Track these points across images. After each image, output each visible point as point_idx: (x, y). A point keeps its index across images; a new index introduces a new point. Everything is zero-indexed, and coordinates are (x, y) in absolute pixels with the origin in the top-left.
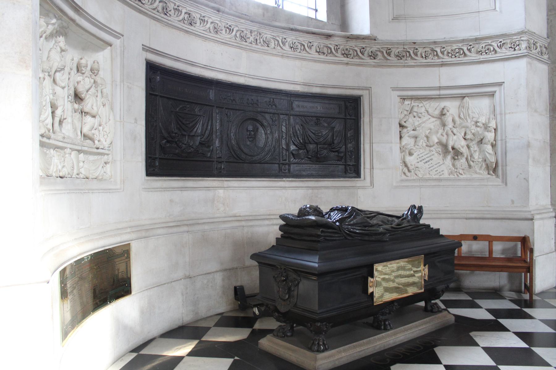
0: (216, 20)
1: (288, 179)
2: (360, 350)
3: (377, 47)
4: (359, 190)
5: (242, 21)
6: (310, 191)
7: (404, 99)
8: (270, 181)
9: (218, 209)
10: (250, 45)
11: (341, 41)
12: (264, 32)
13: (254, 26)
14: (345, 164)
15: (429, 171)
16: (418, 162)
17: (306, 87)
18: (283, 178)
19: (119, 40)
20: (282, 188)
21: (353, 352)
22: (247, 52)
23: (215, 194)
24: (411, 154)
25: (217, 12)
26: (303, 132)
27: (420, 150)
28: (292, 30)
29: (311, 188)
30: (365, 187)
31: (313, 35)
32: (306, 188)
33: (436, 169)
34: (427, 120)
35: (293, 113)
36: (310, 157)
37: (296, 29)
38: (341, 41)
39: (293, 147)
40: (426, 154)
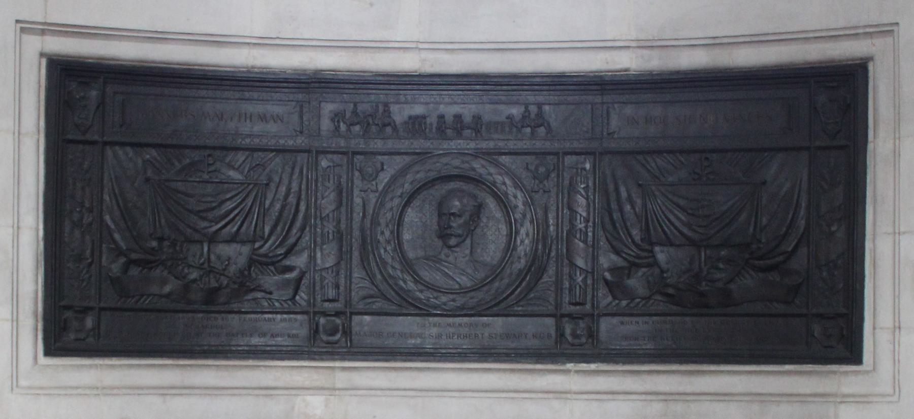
1: (583, 366)
6: (657, 407)
8: (512, 371)
14: (804, 311)
17: (655, 53)
18: (564, 363)
20: (551, 396)
23: (293, 408)
26: (644, 205)
29: (661, 397)
30: (870, 399)
32: (644, 397)
35: (613, 145)
36: (671, 291)
39: (607, 260)
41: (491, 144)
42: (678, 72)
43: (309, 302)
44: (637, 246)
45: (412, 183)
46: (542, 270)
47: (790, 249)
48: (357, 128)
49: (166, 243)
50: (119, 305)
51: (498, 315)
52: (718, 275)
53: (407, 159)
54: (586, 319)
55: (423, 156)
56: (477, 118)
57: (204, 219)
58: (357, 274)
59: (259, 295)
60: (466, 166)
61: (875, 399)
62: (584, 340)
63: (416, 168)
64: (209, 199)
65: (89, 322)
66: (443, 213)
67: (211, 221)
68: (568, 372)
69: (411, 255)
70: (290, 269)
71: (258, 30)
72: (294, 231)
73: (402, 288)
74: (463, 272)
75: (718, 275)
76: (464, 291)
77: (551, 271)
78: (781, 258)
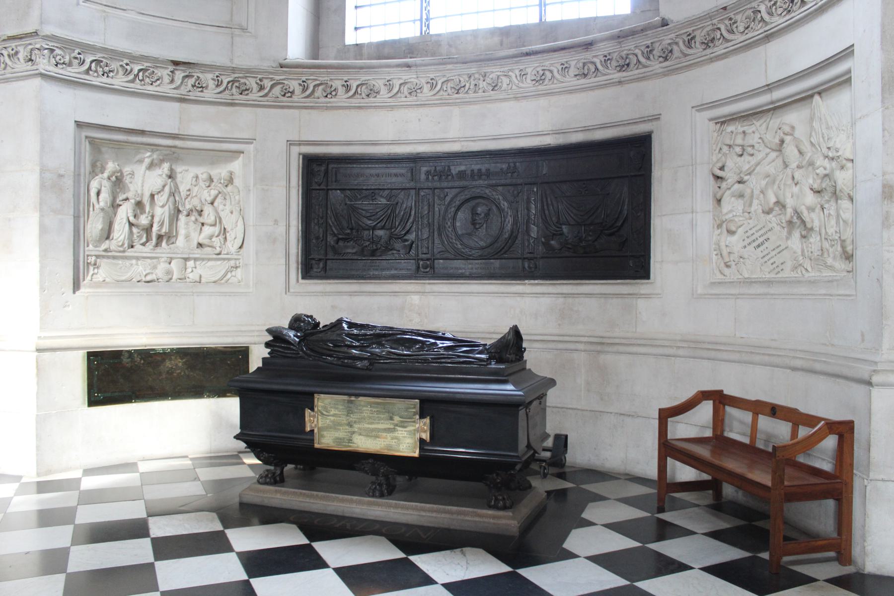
0: (410, 78)
1: (532, 282)
3: (670, 36)
4: (639, 299)
5: (449, 67)
6: (561, 300)
7: (723, 123)
8: (501, 284)
9: (411, 320)
10: (466, 95)
11: (610, 47)
12: (489, 70)
13: (471, 68)
15: (762, 265)
16: (745, 247)
18: (524, 280)
19: (253, 145)
20: (517, 295)
22: (461, 106)
24: (731, 232)
25: (407, 69)
27: (749, 221)
28: (527, 54)
31: (564, 51)
33: (772, 261)
34: (764, 159)
36: (570, 246)
37: (533, 51)
38: (610, 47)
40: (760, 230)
41: (494, 182)
42: (571, 144)
43: (415, 254)
44: (555, 226)
45: (459, 201)
46: (516, 237)
47: (620, 224)
48: (436, 178)
49: (354, 231)
50: (335, 257)
51: (497, 259)
52: (590, 238)
53: (458, 190)
54: (535, 260)
55: (464, 188)
56: (488, 170)
57: (370, 220)
58: (437, 241)
59: (395, 252)
60: (483, 192)
61: (654, 296)
62: (533, 269)
63: (461, 194)
64: (371, 211)
65: (321, 265)
66: (474, 213)
67: (373, 221)
68: (525, 284)
69: (460, 233)
70: (407, 240)
71: (391, 137)
72: (408, 224)
73: (455, 248)
74: (482, 240)
75: (590, 238)
76: (482, 248)
77: (519, 238)
78: (615, 230)
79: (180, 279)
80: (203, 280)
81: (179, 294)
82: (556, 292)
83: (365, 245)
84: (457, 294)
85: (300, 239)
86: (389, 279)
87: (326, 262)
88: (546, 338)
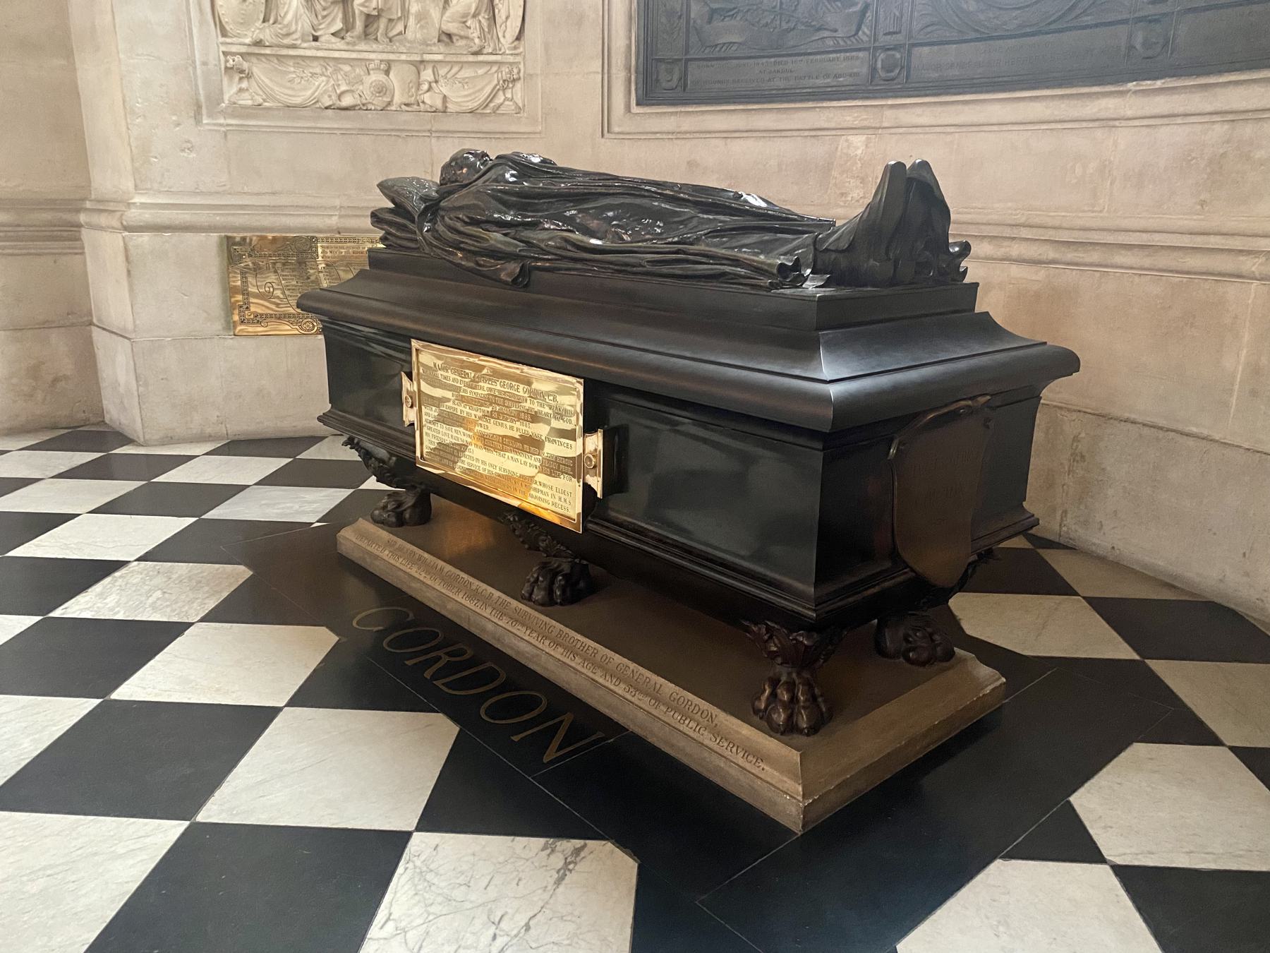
1: (1147, 84)
2: (416, 575)
6: (1220, 130)
8: (1062, 97)
20: (1097, 124)
21: (402, 567)
59: (826, 34)
79: (406, 105)
80: (451, 108)
81: (404, 134)
82: (1209, 108)
83: (763, 22)
84: (949, 129)
85: (634, 14)
86: (808, 100)
87: (686, 67)
88: (1158, 239)
